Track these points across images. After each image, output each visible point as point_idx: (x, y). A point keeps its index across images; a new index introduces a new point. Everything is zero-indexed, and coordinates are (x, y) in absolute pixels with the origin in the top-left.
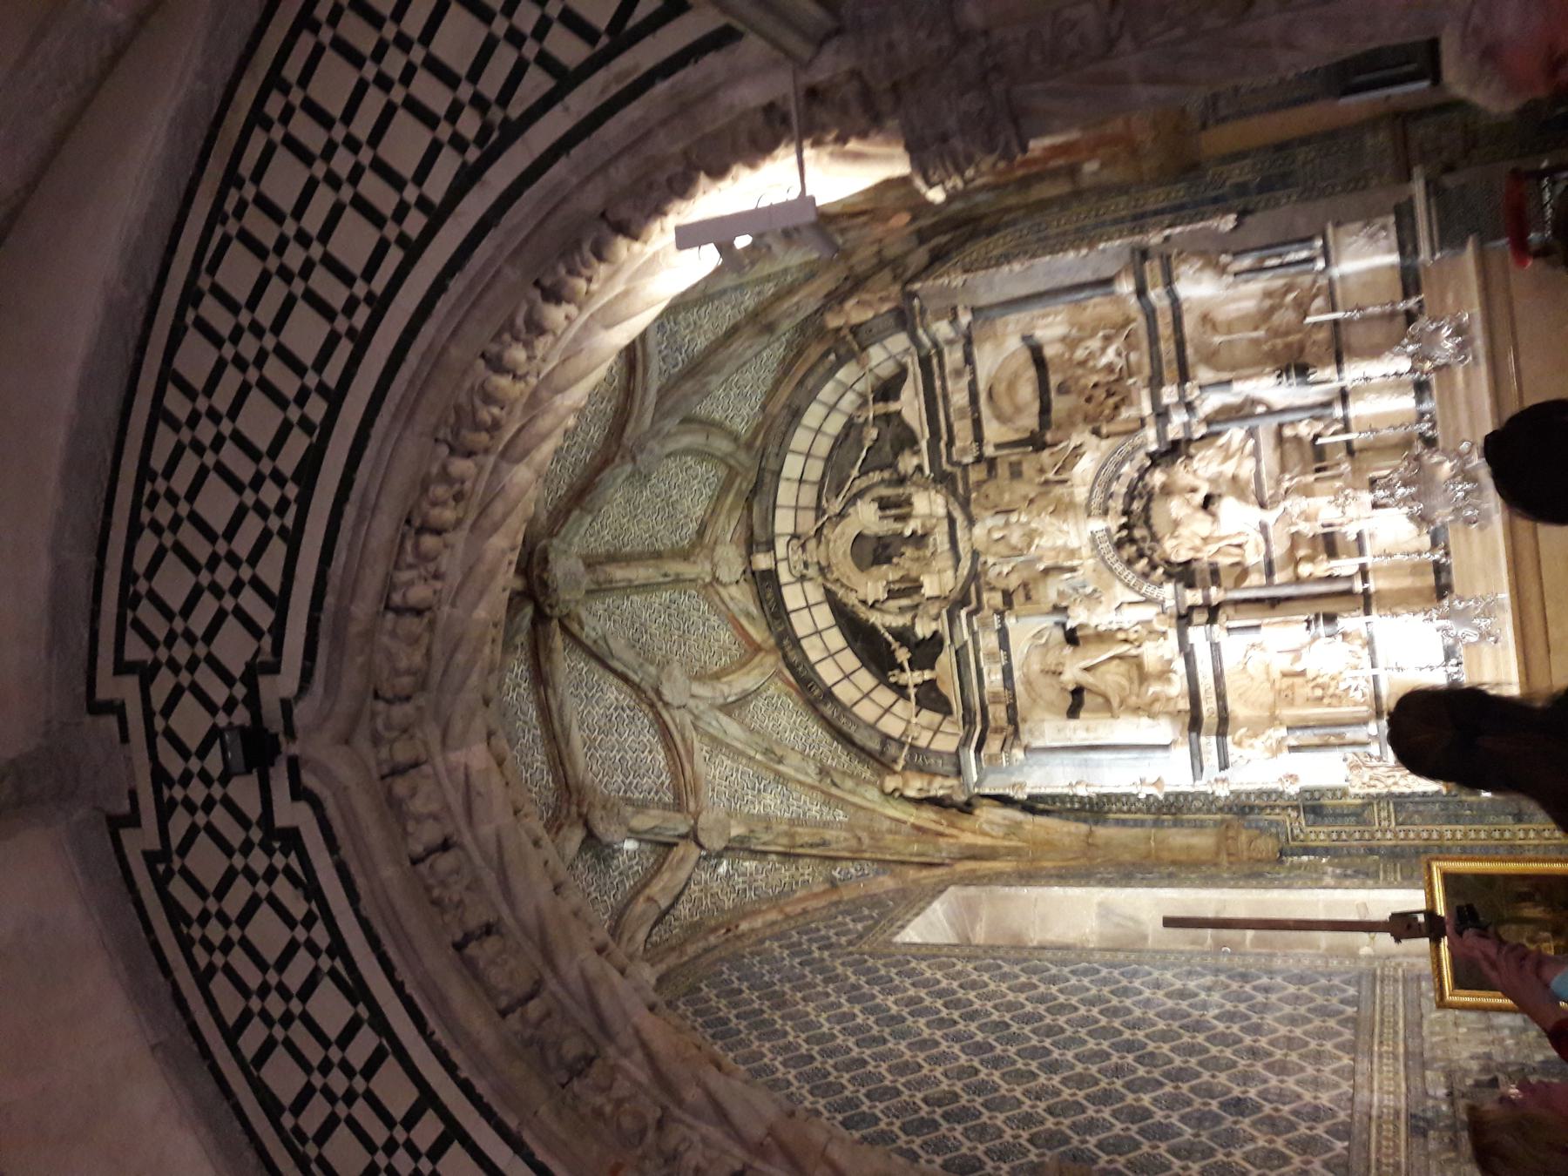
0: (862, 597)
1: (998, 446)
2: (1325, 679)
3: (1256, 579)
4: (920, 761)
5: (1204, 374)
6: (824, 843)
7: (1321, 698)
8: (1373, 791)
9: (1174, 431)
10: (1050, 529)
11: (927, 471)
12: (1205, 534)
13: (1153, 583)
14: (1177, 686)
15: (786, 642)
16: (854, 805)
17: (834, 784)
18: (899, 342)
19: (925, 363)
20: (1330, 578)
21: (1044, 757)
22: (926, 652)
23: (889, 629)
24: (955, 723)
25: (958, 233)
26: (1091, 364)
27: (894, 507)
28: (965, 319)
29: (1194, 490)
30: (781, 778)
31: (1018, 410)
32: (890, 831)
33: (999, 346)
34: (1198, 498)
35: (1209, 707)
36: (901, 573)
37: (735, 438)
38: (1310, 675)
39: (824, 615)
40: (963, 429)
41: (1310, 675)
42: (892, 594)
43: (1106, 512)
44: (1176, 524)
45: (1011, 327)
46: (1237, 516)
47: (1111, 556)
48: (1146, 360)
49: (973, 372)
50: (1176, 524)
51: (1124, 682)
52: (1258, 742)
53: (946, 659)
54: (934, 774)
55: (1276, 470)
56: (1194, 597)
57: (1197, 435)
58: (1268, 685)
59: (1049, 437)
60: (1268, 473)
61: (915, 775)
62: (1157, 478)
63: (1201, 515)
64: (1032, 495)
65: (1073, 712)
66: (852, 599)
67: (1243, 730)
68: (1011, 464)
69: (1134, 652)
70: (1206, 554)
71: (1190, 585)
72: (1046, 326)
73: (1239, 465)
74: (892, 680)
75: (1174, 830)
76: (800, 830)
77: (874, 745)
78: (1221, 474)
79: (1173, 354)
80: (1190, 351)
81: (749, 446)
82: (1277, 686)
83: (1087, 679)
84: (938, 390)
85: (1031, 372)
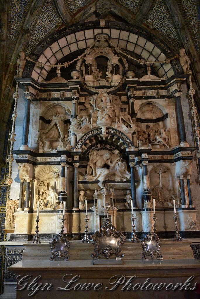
1: (133, 103)
3: (81, 178)
4: (30, 66)
5: (150, 167)
7: (39, 195)
9: (132, 157)
10: (104, 115)
11: (127, 79)
13: (82, 146)
14: (47, 150)
15: (74, 28)
16: (16, 43)
18: (171, 73)
19: (163, 82)
20: (78, 201)
21: (27, 105)
22: (66, 73)
23: (76, 62)
24: (42, 81)
26: (157, 134)
27: (116, 70)
28: (177, 95)
29: (111, 162)
31: (143, 113)
34: (109, 163)
35: (40, 159)
36: (94, 71)
38: (47, 192)
39: (82, 45)
40: (139, 93)
41: (47, 192)
42: (87, 66)
44: (102, 156)
45: (171, 111)
47: (92, 133)
48: (156, 150)
49: (158, 98)
51: (51, 136)
54: (24, 69)
55: (115, 187)
56: (76, 158)
57: (130, 164)
59: (134, 118)
60: (115, 185)
62: (117, 152)
63: (103, 163)
64: (116, 111)
66: (87, 52)
68: (126, 109)
69: (60, 139)
71: (80, 158)
74: (59, 64)
76: (6, 16)
77: (35, 52)
78: (116, 170)
79: (157, 159)
80: (158, 164)
81: (142, 21)
82: (45, 181)
83: (52, 124)
84: (153, 86)
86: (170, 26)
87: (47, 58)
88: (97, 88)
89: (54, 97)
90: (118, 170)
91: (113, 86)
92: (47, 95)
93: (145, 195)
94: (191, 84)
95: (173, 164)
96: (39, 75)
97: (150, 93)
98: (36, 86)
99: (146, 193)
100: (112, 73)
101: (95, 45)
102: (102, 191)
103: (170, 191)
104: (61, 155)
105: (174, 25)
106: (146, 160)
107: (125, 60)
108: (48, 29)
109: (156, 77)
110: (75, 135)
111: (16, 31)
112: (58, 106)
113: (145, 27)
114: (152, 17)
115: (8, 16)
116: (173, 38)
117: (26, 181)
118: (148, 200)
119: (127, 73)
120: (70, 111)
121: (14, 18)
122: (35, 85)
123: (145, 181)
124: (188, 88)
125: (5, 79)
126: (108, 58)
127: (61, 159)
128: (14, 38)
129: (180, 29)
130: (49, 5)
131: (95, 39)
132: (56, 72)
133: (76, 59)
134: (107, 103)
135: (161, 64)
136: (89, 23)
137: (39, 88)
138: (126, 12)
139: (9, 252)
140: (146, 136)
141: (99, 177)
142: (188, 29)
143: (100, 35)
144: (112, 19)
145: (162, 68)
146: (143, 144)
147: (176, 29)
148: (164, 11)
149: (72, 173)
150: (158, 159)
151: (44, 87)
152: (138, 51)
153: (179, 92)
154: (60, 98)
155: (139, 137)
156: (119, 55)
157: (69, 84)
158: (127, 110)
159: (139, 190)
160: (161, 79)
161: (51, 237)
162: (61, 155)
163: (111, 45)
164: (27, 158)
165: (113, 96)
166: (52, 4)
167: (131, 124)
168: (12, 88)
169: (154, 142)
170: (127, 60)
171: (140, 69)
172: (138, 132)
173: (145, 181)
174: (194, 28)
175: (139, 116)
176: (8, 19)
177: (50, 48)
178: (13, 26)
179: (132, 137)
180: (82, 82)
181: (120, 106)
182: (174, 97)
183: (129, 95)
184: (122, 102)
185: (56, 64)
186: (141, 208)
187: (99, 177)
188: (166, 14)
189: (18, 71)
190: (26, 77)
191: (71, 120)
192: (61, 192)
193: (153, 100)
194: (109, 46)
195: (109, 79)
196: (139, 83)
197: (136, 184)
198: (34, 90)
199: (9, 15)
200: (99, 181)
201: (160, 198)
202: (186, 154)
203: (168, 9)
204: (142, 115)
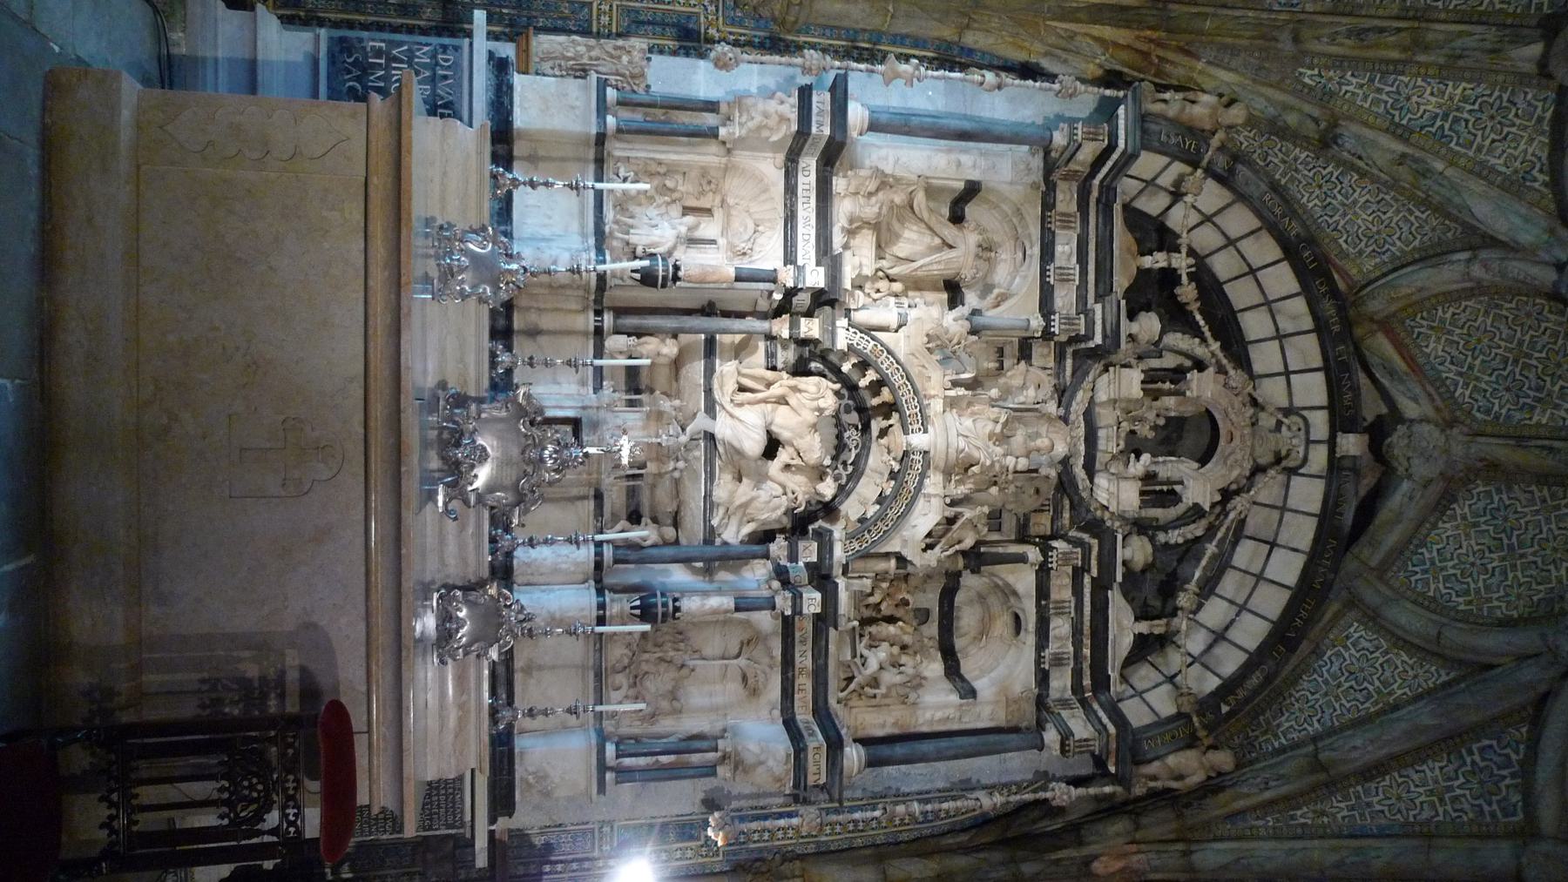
0: (1221, 378)
1: (1021, 559)
2: (660, 200)
4: (1189, 145)
6: (1359, 34)
8: (620, 42)
9: (809, 552)
10: (979, 444)
11: (1120, 537)
12: (783, 408)
14: (843, 210)
15: (1336, 328)
16: (1284, 91)
17: (1316, 121)
18: (1136, 714)
19: (1101, 682)
22: (1154, 292)
23: (1196, 332)
24: (1124, 193)
25: (1026, 829)
26: (896, 650)
27: (1158, 493)
29: (787, 467)
30: (1401, 133)
31: (981, 598)
32: (1234, 51)
33: (1003, 690)
34: (783, 456)
36: (1158, 403)
37: (1373, 618)
39: (1265, 358)
41: (675, 211)
42: (1178, 374)
43: (906, 454)
45: (986, 711)
46: (742, 427)
47: (905, 395)
48: (832, 648)
49: (1039, 660)
50: (814, 427)
51: (896, 226)
52: (758, 119)
53: (1121, 282)
54: (1173, 121)
55: (687, 482)
56: (810, 328)
58: (731, 201)
59: (961, 563)
60: (698, 478)
61: (1198, 124)
62: (827, 489)
63: (784, 434)
64: (994, 490)
65: (972, 190)
66: (1236, 376)
67: (775, 138)
69: (884, 264)
70: (784, 382)
72: (946, 706)
73: (732, 494)
74: (1191, 261)
75: (861, 26)
76: (1395, 55)
80: (777, 652)
83: (950, 232)
84: (1087, 642)
85: (959, 643)
86: (1327, 717)
87: (1215, 214)
88: (1089, 416)
89: (1058, 239)
90: (754, 493)
91: (1092, 482)
92: (1069, 215)
93: (659, 600)
94: (1092, 791)
95: (777, 713)
96: (1150, 183)
97: (1060, 627)
98: (1105, 170)
99: (665, 605)
100: (1149, 477)
101: (1263, 409)
102: (674, 429)
103: (673, 695)
104: (822, 270)
105: (1331, 732)
106: (794, 606)
107: (1199, 533)
108: (1337, 223)
109: (1125, 654)
110: (900, 326)
111: (1332, 94)
112: (1020, 255)
113: (1328, 616)
114: (1366, 645)
115: (1395, 62)
116: (1279, 726)
117: (724, 125)
118: (638, 612)
119: (1146, 539)
120: (998, 305)
121: (1388, 89)
122: (1110, 164)
123: (714, 602)
124: (1077, 782)
125: (1138, 38)
126: (1209, 466)
127: (808, 269)
128: (1305, 85)
129: (1316, 756)
130: (1433, 229)
131: (1288, 411)
132: (1160, 250)
133: (1208, 334)
134: (1027, 456)
135: (1175, 675)
136: (1356, 390)
137: (1096, 182)
138: (1392, 539)
139: (444, 52)
140: (886, 609)
141: (731, 416)
142: (1313, 789)
143: (1302, 433)
144: (1365, 482)
145: (1162, 679)
146: (859, 598)
147: (1315, 739)
148: (1390, 694)
149: (749, 309)
150: (797, 655)
151: (1098, 201)
152: (1230, 584)
153: (1063, 745)
154: (1051, 267)
155: (884, 580)
156: (1218, 509)
157: (1108, 306)
158: (995, 537)
159: (678, 576)
160: (1113, 674)
161: (499, 223)
162: (822, 270)
163: (1260, 480)
164: (814, 130)
165: (1054, 480)
166: (1439, 244)
167: (937, 549)
168: (1100, 66)
169: (865, 640)
170: (1197, 539)
171: (1158, 591)
172: (906, 577)
173: (714, 602)
174: (1315, 812)
175: (969, 581)
176: (1382, 61)
177: (1259, 229)
178: (1354, 81)
179: (887, 555)
180: (1113, 358)
181: (1009, 507)
182: (1040, 726)
183: (1055, 544)
184: (1027, 518)
185: (1191, 252)
186: (609, 580)
187: (731, 416)
188: (1376, 703)
189: (1167, 96)
190: (1144, 131)
191: (961, 311)
192: (677, 268)
193: (1030, 639)
194: (1258, 470)
195: (1121, 467)
196: (1101, 587)
197: (700, 565)
198: (1090, 159)
199: (1398, 67)
200: (714, 418)
201: (646, 656)
202: (817, 763)
203: (1396, 707)
204: (972, 594)
